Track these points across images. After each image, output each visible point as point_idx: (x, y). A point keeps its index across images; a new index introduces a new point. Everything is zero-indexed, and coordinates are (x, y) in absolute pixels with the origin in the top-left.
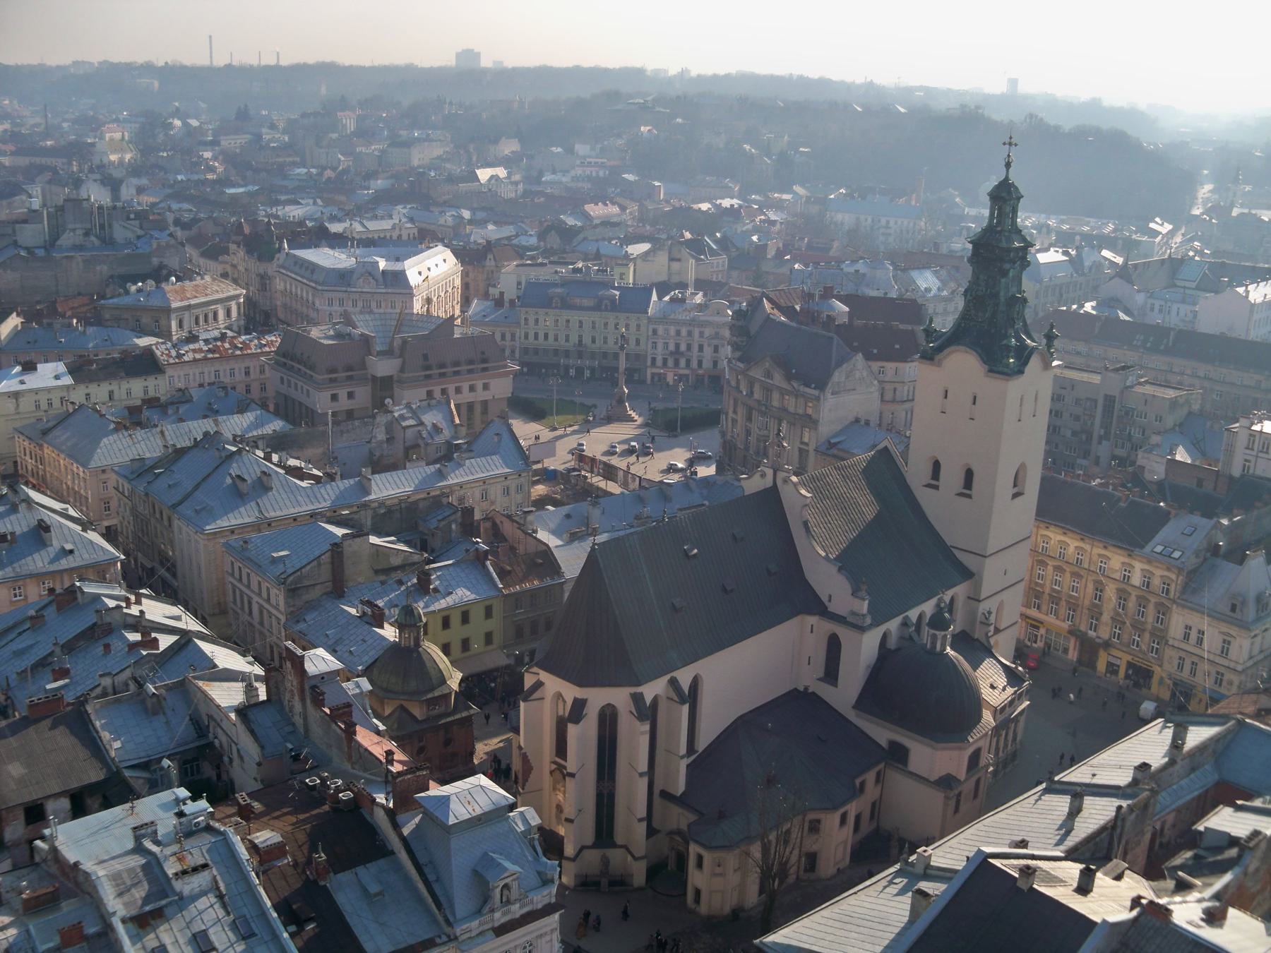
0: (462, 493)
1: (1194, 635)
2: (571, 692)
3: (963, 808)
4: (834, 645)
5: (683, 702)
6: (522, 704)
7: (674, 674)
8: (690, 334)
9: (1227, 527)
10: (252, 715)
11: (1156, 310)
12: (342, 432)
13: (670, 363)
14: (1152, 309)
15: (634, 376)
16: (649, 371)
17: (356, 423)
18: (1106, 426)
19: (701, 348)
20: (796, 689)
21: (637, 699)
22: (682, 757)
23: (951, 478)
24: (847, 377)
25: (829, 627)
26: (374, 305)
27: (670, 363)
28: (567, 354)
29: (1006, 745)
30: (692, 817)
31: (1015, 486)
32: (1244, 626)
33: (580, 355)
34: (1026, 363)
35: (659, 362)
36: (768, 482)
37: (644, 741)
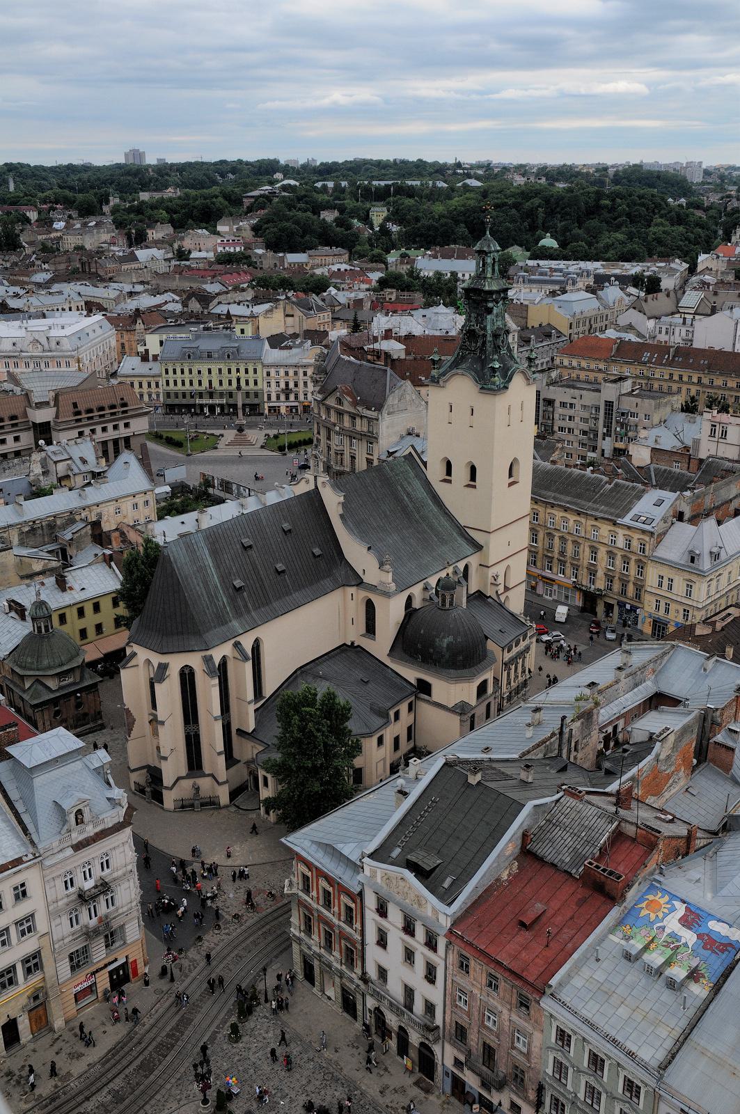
0: (99, 511)
2: (156, 659)
4: (370, 606)
5: (246, 659)
6: (123, 672)
7: (238, 639)
9: (690, 498)
11: (664, 331)
12: (4, 469)
14: (660, 332)
15: (253, 409)
16: (266, 406)
17: (16, 461)
18: (608, 425)
19: (305, 383)
20: (344, 644)
21: (208, 660)
22: (249, 703)
25: (363, 594)
26: (43, 365)
27: (283, 397)
28: (201, 395)
29: (517, 677)
30: (261, 748)
31: (510, 475)
32: (701, 574)
33: (211, 395)
34: (510, 379)
35: (274, 398)
36: (313, 487)
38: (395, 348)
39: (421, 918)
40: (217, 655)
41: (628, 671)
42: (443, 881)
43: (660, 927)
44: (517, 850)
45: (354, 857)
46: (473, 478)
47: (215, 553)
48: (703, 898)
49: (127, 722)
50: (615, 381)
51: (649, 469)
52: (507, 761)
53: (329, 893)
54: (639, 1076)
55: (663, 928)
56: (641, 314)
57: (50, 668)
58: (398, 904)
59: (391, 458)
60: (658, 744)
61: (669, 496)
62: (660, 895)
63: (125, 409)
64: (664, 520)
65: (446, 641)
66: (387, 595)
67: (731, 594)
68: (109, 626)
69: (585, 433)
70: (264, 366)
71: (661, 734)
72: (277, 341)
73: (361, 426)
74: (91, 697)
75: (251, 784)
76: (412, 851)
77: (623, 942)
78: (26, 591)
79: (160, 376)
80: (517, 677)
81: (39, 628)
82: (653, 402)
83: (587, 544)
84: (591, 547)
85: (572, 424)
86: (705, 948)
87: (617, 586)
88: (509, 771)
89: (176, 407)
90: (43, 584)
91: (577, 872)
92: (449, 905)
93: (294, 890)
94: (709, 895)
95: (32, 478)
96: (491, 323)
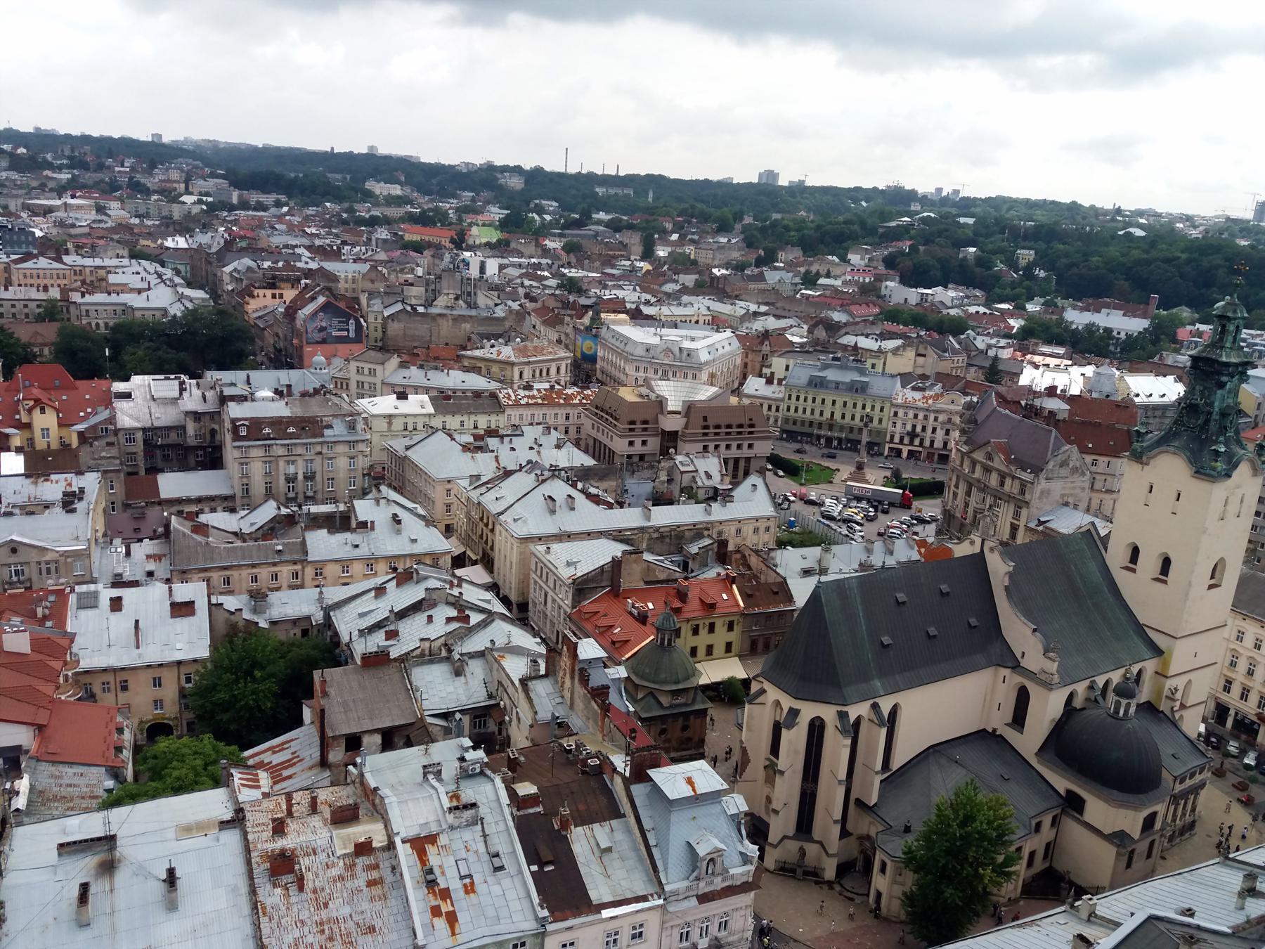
2: (787, 702)
3: (1134, 865)
4: (1023, 698)
5: (881, 724)
6: (746, 705)
7: (876, 700)
8: (926, 418)
10: (531, 684)
13: (906, 440)
16: (887, 446)
19: (934, 430)
20: (984, 730)
21: (843, 716)
22: (877, 773)
25: (1018, 679)
26: (670, 374)
27: (906, 440)
28: (820, 425)
29: (1184, 814)
30: (881, 828)
31: (1212, 577)
33: (831, 427)
34: (1236, 466)
35: (897, 440)
37: (846, 753)
40: (854, 712)
57: (665, 682)
59: (1041, 528)
66: (1048, 686)
68: (719, 649)
72: (906, 378)
73: (1010, 487)
74: (698, 721)
80: (1184, 814)
81: (663, 640)
89: (793, 433)
96: (1219, 400)
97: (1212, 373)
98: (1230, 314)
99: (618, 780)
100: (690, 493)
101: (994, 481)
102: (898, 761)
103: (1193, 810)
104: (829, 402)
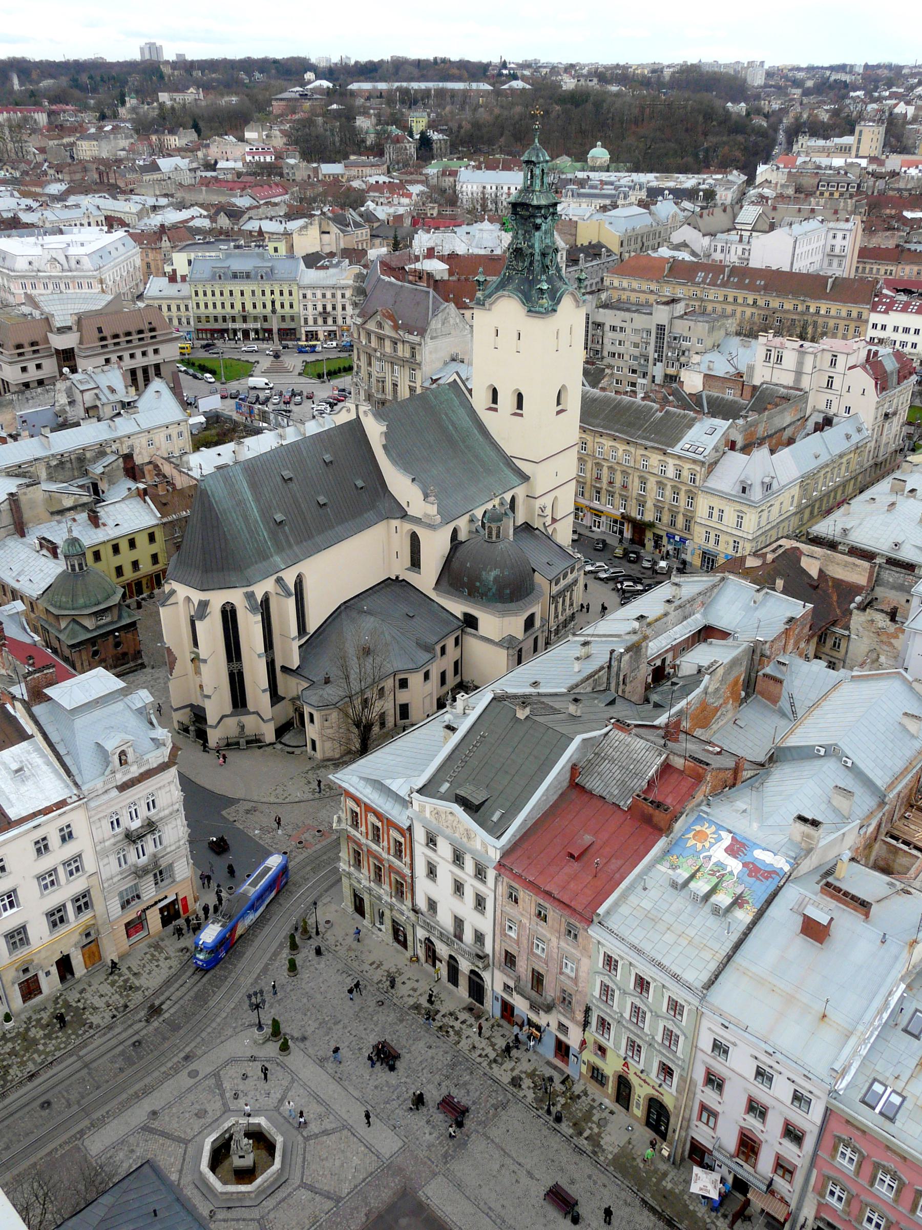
0: (130, 443)
1: (716, 513)
2: (197, 596)
4: (415, 540)
5: (289, 595)
7: (279, 574)
8: (333, 296)
9: (743, 426)
14: (715, 250)
17: (39, 390)
18: (659, 349)
19: (344, 308)
21: (250, 596)
22: (293, 639)
23: (507, 401)
24: (443, 324)
25: (408, 527)
26: (63, 286)
27: (320, 321)
28: (234, 319)
30: (306, 685)
31: (558, 403)
32: (752, 505)
35: (311, 322)
38: (437, 267)
39: (472, 852)
40: (259, 591)
41: (677, 603)
42: (493, 814)
43: (705, 857)
44: (565, 784)
45: (403, 793)
46: (520, 405)
47: (254, 486)
48: (749, 828)
49: (169, 660)
50: (667, 303)
51: (701, 396)
52: (556, 695)
53: (378, 828)
54: (682, 996)
55: (710, 857)
56: (696, 231)
58: (447, 838)
59: (434, 386)
60: (707, 677)
61: (722, 425)
62: (707, 825)
63: (153, 334)
64: (716, 449)
65: (493, 574)
66: (432, 527)
67: (782, 526)
69: (636, 358)
70: (300, 287)
71: (709, 667)
72: (312, 260)
73: (403, 351)
74: (130, 635)
75: (296, 722)
76: (460, 786)
77: (670, 872)
78: (57, 528)
79: (190, 298)
81: (73, 566)
82: (707, 325)
83: (637, 474)
84: (640, 477)
85: (621, 349)
86: (750, 875)
87: (666, 518)
88: (557, 706)
90: (74, 520)
91: (626, 803)
92: (498, 838)
93: (343, 826)
94: (755, 825)
95: (57, 408)
96: (538, 241)
97: (529, 217)
98: (534, 159)
99: (18, 705)
100: (92, 411)
101: (388, 348)
102: (312, 627)
103: (571, 605)
104: (237, 293)
